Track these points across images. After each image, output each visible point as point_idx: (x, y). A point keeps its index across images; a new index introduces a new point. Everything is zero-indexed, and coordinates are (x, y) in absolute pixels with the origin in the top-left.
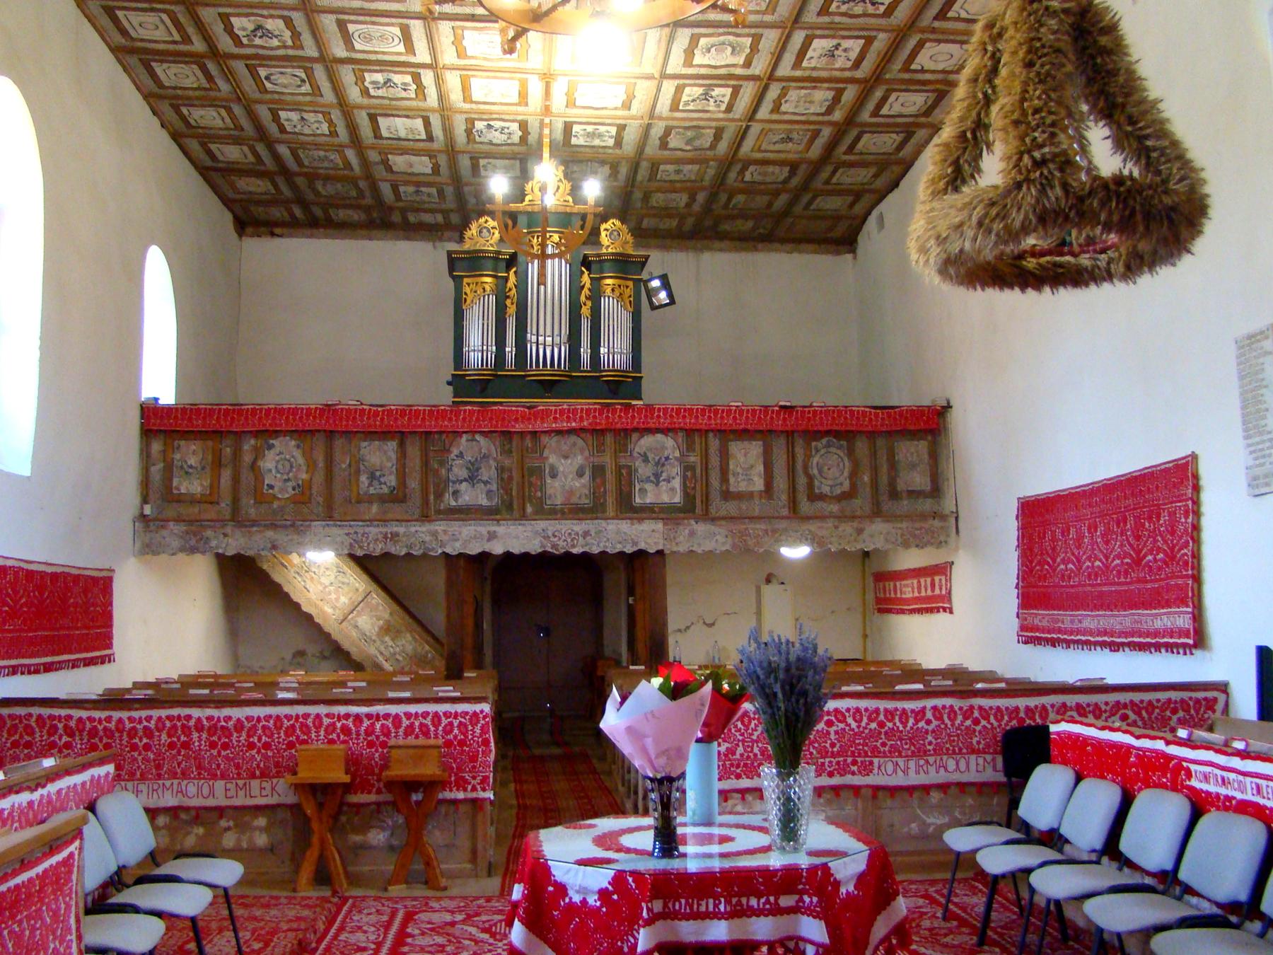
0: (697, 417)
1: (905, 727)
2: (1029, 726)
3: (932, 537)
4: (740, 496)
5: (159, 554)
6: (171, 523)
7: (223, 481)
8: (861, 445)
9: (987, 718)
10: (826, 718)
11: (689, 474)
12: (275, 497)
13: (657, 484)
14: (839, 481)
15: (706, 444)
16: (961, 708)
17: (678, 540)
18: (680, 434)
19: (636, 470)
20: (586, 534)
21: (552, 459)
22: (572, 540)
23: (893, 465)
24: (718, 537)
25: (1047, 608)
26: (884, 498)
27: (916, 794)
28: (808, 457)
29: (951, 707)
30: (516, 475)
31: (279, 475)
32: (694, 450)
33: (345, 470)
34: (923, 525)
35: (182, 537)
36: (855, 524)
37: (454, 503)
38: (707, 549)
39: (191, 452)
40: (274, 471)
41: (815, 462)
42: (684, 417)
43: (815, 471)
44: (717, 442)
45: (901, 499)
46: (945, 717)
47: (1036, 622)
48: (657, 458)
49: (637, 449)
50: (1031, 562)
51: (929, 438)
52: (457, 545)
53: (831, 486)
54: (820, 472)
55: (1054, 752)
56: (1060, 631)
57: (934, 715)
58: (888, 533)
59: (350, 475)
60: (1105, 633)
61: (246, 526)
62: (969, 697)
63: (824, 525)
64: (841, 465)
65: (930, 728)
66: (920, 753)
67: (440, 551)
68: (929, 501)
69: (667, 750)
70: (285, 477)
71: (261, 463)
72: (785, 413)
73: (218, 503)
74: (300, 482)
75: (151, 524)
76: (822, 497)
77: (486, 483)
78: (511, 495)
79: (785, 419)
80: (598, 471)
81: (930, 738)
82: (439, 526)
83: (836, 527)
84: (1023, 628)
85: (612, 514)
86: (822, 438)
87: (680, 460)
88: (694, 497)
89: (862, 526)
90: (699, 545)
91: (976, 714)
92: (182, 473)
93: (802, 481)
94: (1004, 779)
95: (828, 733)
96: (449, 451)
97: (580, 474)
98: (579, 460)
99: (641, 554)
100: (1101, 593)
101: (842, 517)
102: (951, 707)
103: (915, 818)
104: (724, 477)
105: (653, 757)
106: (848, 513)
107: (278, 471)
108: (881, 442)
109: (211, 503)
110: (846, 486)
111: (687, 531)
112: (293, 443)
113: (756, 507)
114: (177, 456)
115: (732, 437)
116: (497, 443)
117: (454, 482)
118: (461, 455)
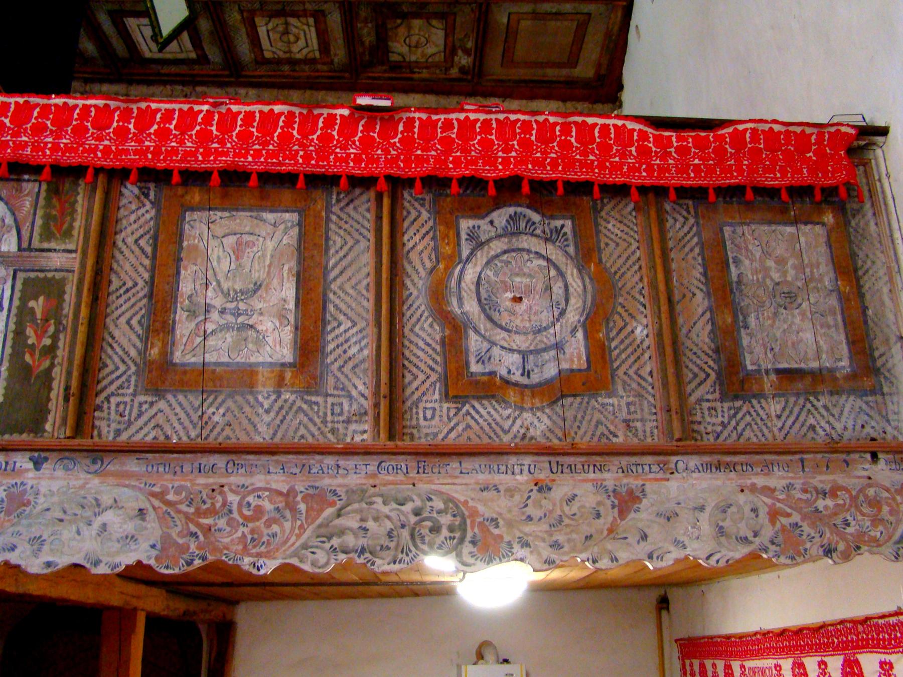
0: (80, 132)
3: (876, 521)
11: (38, 305)
14: (548, 338)
24: (109, 516)
34: (841, 479)
36: (610, 478)
38: (63, 561)
41: (471, 274)
42: (39, 129)
43: (471, 307)
44: (148, 212)
51: (829, 218)
53: (524, 355)
54: (487, 307)
63: (497, 478)
64: (558, 289)
68: (850, 404)
72: (369, 127)
79: (367, 143)
83: (542, 487)
86: (497, 205)
88: (47, 377)
89: (634, 483)
90: (38, 542)
106: (584, 438)
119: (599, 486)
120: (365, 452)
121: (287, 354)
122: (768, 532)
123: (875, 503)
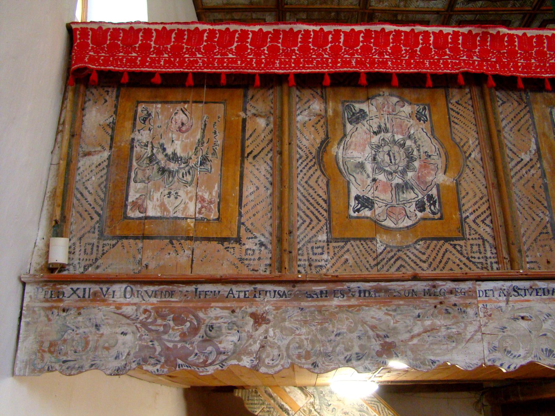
5: (80, 370)
6: (119, 288)
7: (248, 189)
12: (376, 224)
31: (382, 177)
33: (530, 165)
35: (144, 324)
39: (174, 127)
40: (369, 167)
59: (544, 176)
61: (310, 295)
70: (397, 180)
71: (336, 150)
73: (238, 240)
74: (434, 192)
75: (67, 289)
92: (152, 171)
107: (379, 168)
109: (222, 240)
112: (407, 109)
114: (144, 136)
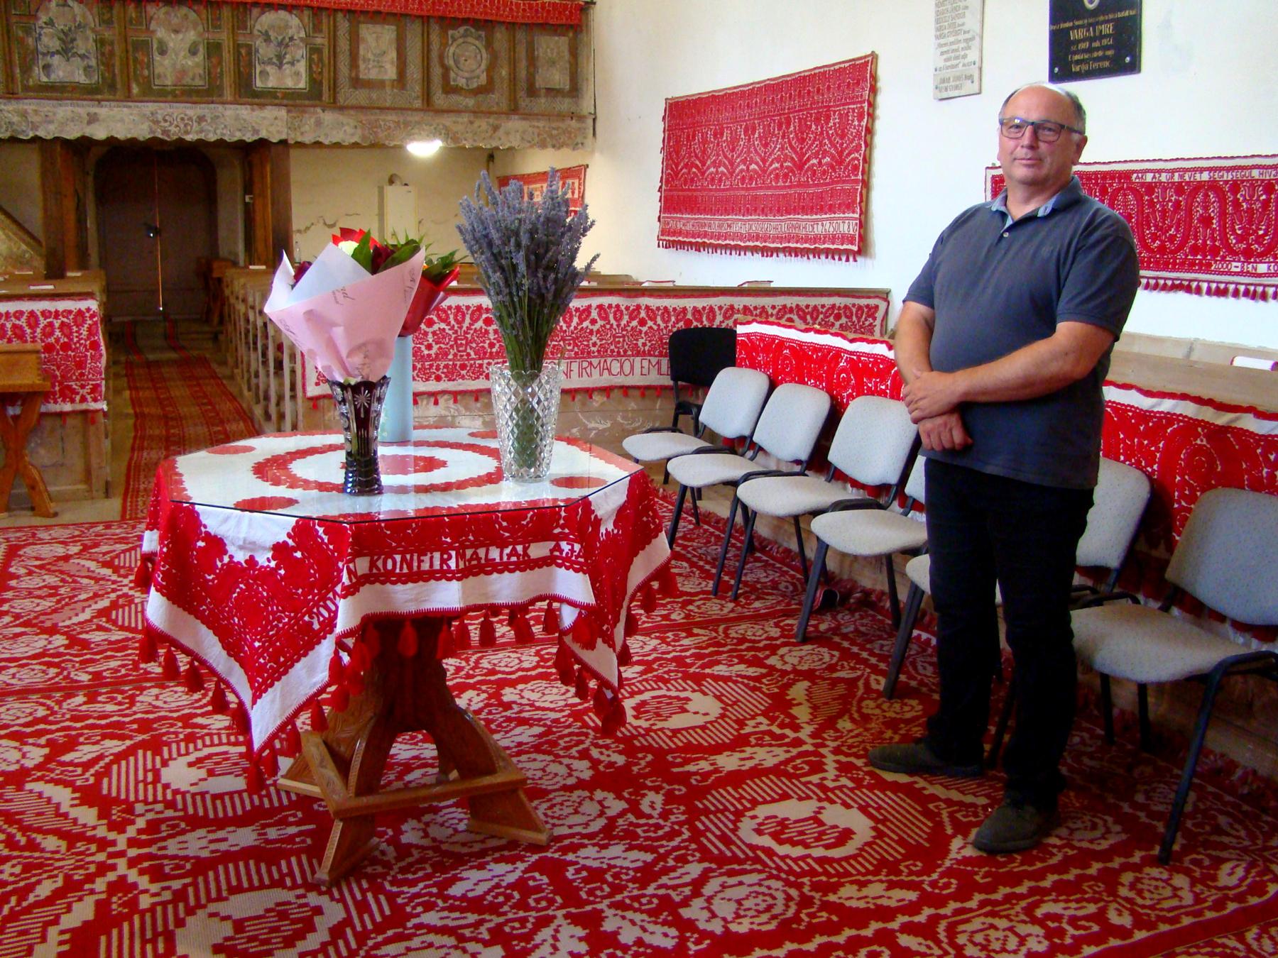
1: (568, 327)
2: (696, 327)
4: (369, 84)
8: (500, 36)
9: (654, 319)
10: (484, 316)
11: (315, 57)
13: (280, 66)
15: (335, 26)
16: (627, 308)
17: (303, 129)
18: (306, 12)
19: (257, 51)
20: (201, 119)
21: (161, 33)
22: (186, 125)
23: (532, 61)
25: (692, 212)
26: (521, 94)
27: (578, 397)
28: (444, 45)
29: (618, 306)
30: (118, 50)
32: (321, 31)
36: (491, 121)
37: (44, 79)
43: (451, 63)
44: (347, 24)
45: (539, 96)
46: (611, 317)
47: (680, 225)
48: (280, 38)
49: (258, 27)
50: (677, 165)
51: (571, 35)
52: (52, 127)
53: (467, 79)
54: (456, 62)
55: (740, 354)
56: (705, 235)
57: (599, 315)
58: (524, 132)
60: (757, 238)
62: (636, 296)
63: (460, 120)
65: (595, 328)
66: (584, 354)
67: (31, 134)
68: (567, 100)
69: (364, 344)
76: (456, 90)
77: (83, 57)
78: (114, 75)
80: (213, 49)
81: (594, 339)
82: (29, 106)
83: (471, 123)
84: (663, 232)
85: (230, 98)
86: (460, 25)
87: (307, 41)
88: (321, 83)
89: (496, 122)
90: (327, 135)
91: (643, 314)
93: (437, 71)
94: (671, 383)
95: (487, 332)
96: (36, 17)
97: (193, 52)
98: (192, 36)
99: (263, 143)
100: (756, 198)
101: (476, 112)
102: (618, 306)
103: (576, 423)
104: (354, 63)
105: (344, 353)
106: (483, 108)
108: (521, 35)
110: (483, 79)
111: (313, 120)
113: (388, 97)
115: (362, 18)
116: (95, 10)
117: (44, 55)
118: (50, 23)
119: (488, 123)
120: (416, 110)
121: (394, 77)
122: (536, 139)
123: (570, 133)
